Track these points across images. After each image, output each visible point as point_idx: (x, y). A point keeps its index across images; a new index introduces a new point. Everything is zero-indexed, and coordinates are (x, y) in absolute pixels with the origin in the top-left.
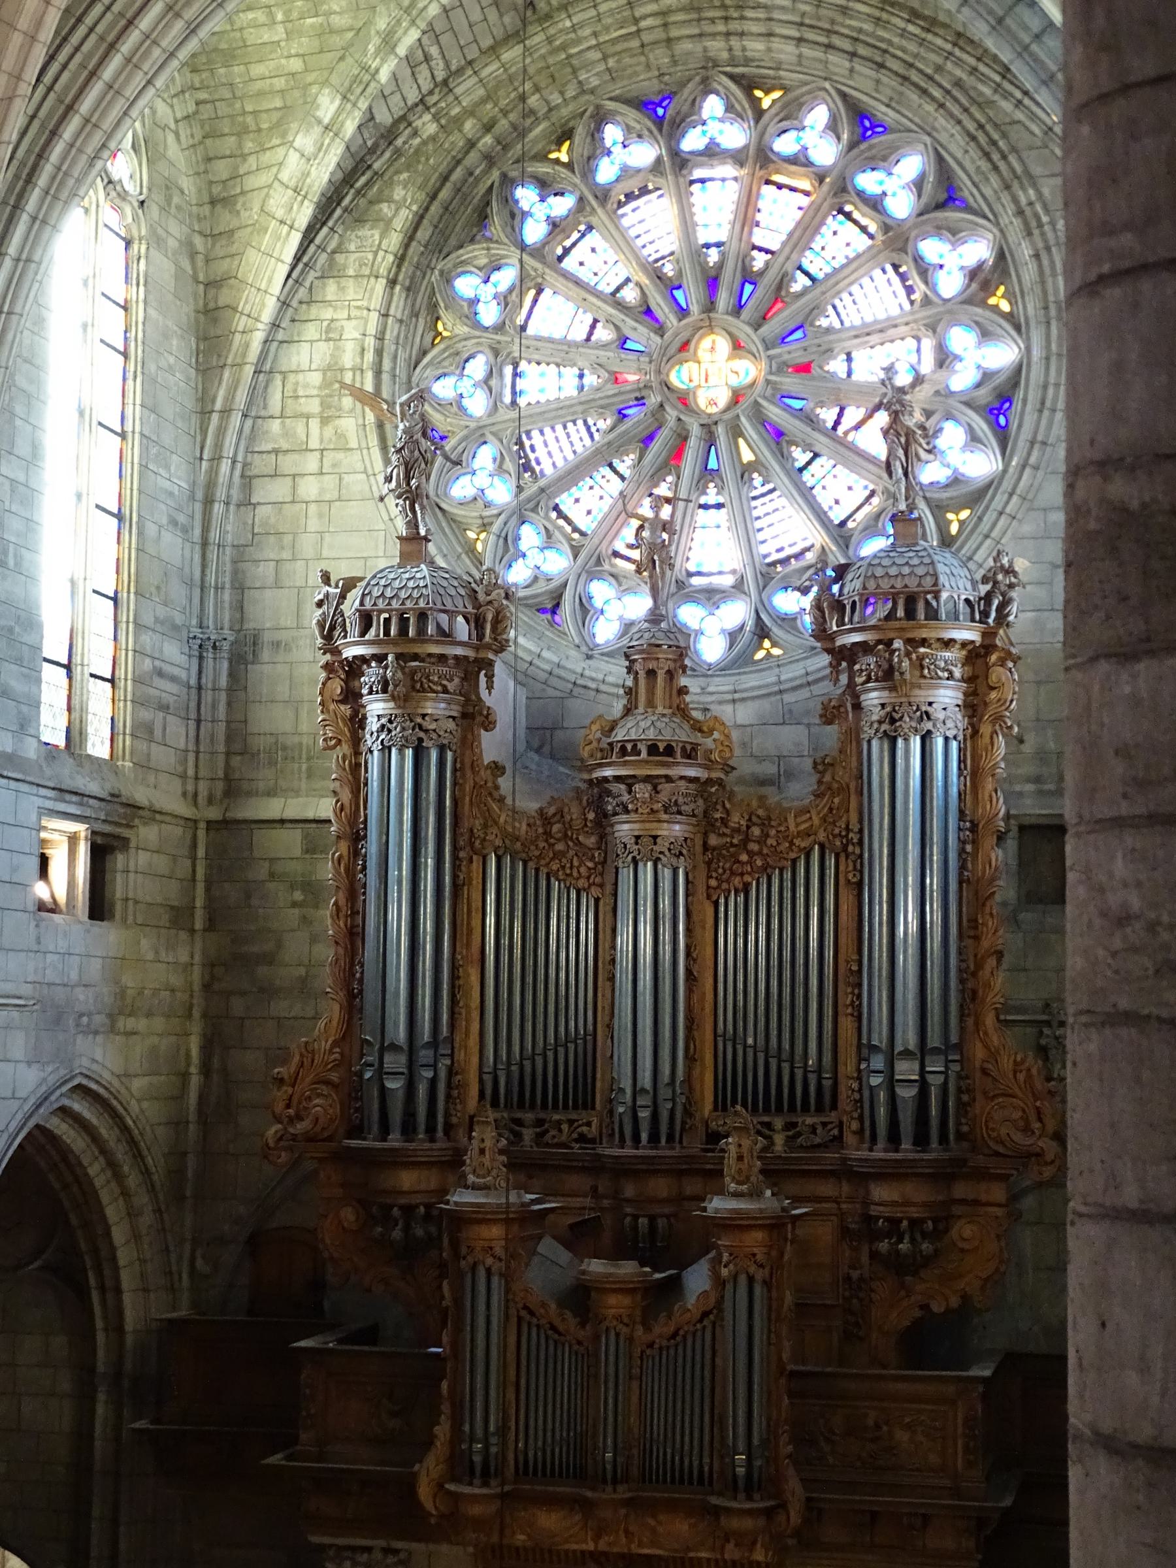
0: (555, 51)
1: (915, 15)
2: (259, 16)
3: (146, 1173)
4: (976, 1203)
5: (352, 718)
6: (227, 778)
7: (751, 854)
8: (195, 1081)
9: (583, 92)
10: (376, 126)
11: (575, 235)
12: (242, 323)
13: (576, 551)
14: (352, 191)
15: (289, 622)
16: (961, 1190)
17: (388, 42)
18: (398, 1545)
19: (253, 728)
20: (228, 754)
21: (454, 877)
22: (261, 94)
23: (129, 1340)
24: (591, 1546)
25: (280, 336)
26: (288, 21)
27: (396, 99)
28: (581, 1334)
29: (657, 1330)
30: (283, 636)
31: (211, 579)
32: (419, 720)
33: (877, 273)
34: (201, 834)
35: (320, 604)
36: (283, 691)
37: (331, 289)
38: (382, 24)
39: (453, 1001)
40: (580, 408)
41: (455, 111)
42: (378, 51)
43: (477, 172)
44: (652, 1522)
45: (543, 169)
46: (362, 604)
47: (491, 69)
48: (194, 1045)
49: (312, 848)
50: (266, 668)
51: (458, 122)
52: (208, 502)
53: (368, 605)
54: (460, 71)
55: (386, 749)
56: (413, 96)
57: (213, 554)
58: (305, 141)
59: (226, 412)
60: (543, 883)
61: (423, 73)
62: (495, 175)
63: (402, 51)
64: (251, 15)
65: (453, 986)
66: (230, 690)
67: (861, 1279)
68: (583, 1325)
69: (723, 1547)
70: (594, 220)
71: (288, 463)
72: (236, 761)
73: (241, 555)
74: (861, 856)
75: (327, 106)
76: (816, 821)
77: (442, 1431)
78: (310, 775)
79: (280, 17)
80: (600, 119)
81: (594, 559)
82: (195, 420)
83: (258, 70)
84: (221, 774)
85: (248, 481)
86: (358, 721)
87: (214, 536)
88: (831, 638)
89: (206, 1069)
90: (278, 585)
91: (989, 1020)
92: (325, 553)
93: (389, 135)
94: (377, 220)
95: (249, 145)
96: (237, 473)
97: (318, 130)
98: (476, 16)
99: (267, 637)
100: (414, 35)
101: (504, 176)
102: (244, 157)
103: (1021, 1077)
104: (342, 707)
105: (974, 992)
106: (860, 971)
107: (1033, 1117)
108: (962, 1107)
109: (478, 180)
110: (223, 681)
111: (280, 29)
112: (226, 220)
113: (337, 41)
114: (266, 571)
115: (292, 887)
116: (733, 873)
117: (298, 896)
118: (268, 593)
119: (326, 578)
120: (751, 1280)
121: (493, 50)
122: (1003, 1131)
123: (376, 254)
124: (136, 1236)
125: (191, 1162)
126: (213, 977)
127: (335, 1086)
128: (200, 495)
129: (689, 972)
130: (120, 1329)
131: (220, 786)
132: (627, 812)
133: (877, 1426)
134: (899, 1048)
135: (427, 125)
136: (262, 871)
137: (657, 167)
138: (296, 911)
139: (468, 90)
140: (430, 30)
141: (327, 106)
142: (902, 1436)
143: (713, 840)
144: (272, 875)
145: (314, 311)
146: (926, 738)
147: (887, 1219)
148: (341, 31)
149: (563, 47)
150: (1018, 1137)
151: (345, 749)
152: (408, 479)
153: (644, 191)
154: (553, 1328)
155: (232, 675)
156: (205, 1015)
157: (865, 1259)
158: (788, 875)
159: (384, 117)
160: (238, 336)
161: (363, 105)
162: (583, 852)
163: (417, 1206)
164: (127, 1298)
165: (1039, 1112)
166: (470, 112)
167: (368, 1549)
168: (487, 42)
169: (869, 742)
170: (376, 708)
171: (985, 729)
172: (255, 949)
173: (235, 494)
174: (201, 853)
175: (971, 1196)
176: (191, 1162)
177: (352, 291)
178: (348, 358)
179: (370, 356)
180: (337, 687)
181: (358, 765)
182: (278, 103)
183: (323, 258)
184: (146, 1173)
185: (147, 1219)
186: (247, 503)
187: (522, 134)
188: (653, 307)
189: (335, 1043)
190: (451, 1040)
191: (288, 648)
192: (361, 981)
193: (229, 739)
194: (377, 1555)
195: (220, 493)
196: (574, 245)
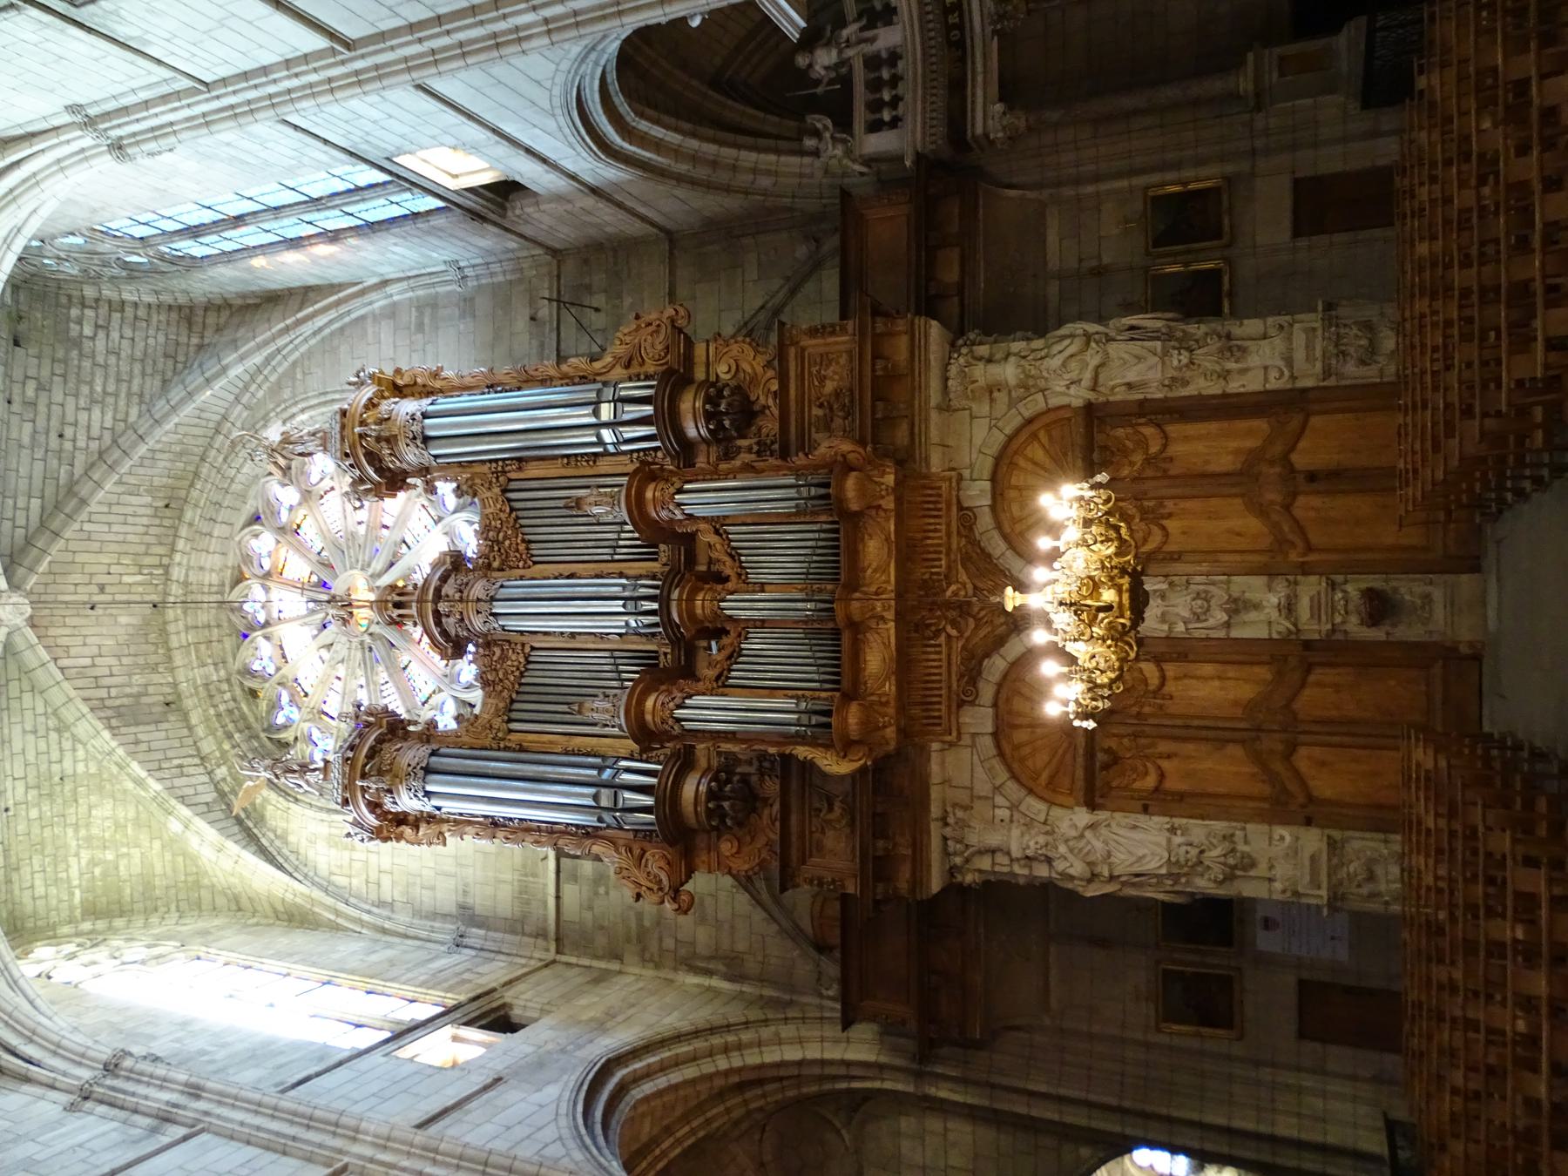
0: (197, 693)
1: (192, 485)
2: (123, 863)
3: (747, 1024)
4: (708, 365)
6: (537, 936)
7: (505, 538)
8: (715, 982)
9: (228, 681)
10: (215, 801)
12: (289, 897)
13: (440, 690)
15: (452, 881)
16: (700, 374)
17: (139, 782)
18: (935, 811)
19: (509, 915)
20: (524, 934)
21: (514, 750)
22: (174, 871)
23: (883, 1059)
24: (892, 624)
25: (311, 874)
26: (128, 845)
27: (200, 789)
28: (733, 634)
29: (728, 571)
30: (460, 888)
31: (424, 934)
33: (322, 508)
34: (564, 958)
36: (489, 890)
37: (292, 839)
38: (130, 785)
39: (588, 755)
41: (217, 754)
42: (145, 789)
44: (869, 571)
45: (263, 705)
47: (200, 731)
48: (693, 980)
49: (575, 878)
50: (478, 901)
51: (224, 753)
52: (384, 931)
54: (198, 750)
55: (428, 794)
56: (205, 779)
57: (412, 932)
58: (194, 843)
59: (338, 913)
60: (524, 689)
61: (191, 770)
62: (263, 735)
63: (144, 774)
64: (122, 868)
65: (574, 754)
66: (488, 929)
67: (758, 443)
68: (727, 633)
69: (885, 511)
70: (291, 677)
71: (373, 877)
72: (528, 929)
73: (417, 913)
74: (504, 460)
75: (175, 826)
76: (489, 494)
77: (802, 752)
78: (534, 875)
79: (124, 850)
80: (248, 672)
82: (340, 934)
83: (158, 869)
84: (532, 940)
85: (381, 904)
86: (430, 819)
87: (401, 929)
88: (377, 485)
89: (709, 973)
90: (433, 888)
91: (597, 365)
93: (222, 795)
95: (206, 881)
96: (375, 910)
97: (188, 834)
98: (163, 734)
99: (461, 899)
100: (135, 765)
101: (264, 730)
102: (213, 886)
103: (628, 339)
105: (582, 377)
106: (568, 456)
107: (650, 329)
108: (647, 378)
109: (263, 746)
110: (482, 932)
111: (132, 851)
112: (245, 903)
113: (144, 816)
114: (427, 896)
115: (596, 893)
116: (517, 550)
117: (602, 890)
118: (439, 895)
119: (349, 835)
120: (680, 491)
121: (190, 728)
122: (659, 347)
124: (801, 1041)
125: (769, 992)
126: (651, 960)
127: (644, 852)
128: (379, 936)
129: (568, 577)
130: (880, 1067)
131: (540, 942)
132: (462, 620)
133: (821, 406)
134: (593, 420)
135: (222, 772)
136: (588, 916)
137: (267, 638)
138: (612, 893)
139: (208, 746)
140: (132, 754)
141: (175, 826)
142: (830, 386)
143: (496, 564)
144: (590, 908)
145: (302, 851)
146: (425, 416)
147: (707, 423)
148: (138, 812)
149: (196, 688)
150: (662, 337)
151: (445, 827)
152: (294, 771)
153: (281, 647)
154: (730, 657)
155: (479, 927)
156: (675, 969)
157: (744, 443)
158: (520, 514)
159: (210, 797)
160: (298, 900)
161: (173, 802)
162: (504, 658)
163: (709, 789)
164: (851, 1056)
165: (650, 324)
166: (220, 745)
167: (945, 839)
168: (185, 732)
169: (436, 457)
170: (407, 802)
171: (438, 384)
172: (634, 926)
173: (385, 913)
174: (573, 960)
175: (703, 369)
176: (769, 992)
177: (293, 826)
178: (324, 830)
179: (324, 816)
180: (408, 831)
181: (455, 821)
182: (180, 859)
183: (278, 843)
184: (747, 1024)
185: (788, 1031)
186: (390, 905)
187: (243, 717)
188: (329, 642)
189: (617, 851)
190: (604, 757)
191: (466, 885)
192: (577, 826)
193: (513, 932)
194: (948, 831)
195: (379, 922)
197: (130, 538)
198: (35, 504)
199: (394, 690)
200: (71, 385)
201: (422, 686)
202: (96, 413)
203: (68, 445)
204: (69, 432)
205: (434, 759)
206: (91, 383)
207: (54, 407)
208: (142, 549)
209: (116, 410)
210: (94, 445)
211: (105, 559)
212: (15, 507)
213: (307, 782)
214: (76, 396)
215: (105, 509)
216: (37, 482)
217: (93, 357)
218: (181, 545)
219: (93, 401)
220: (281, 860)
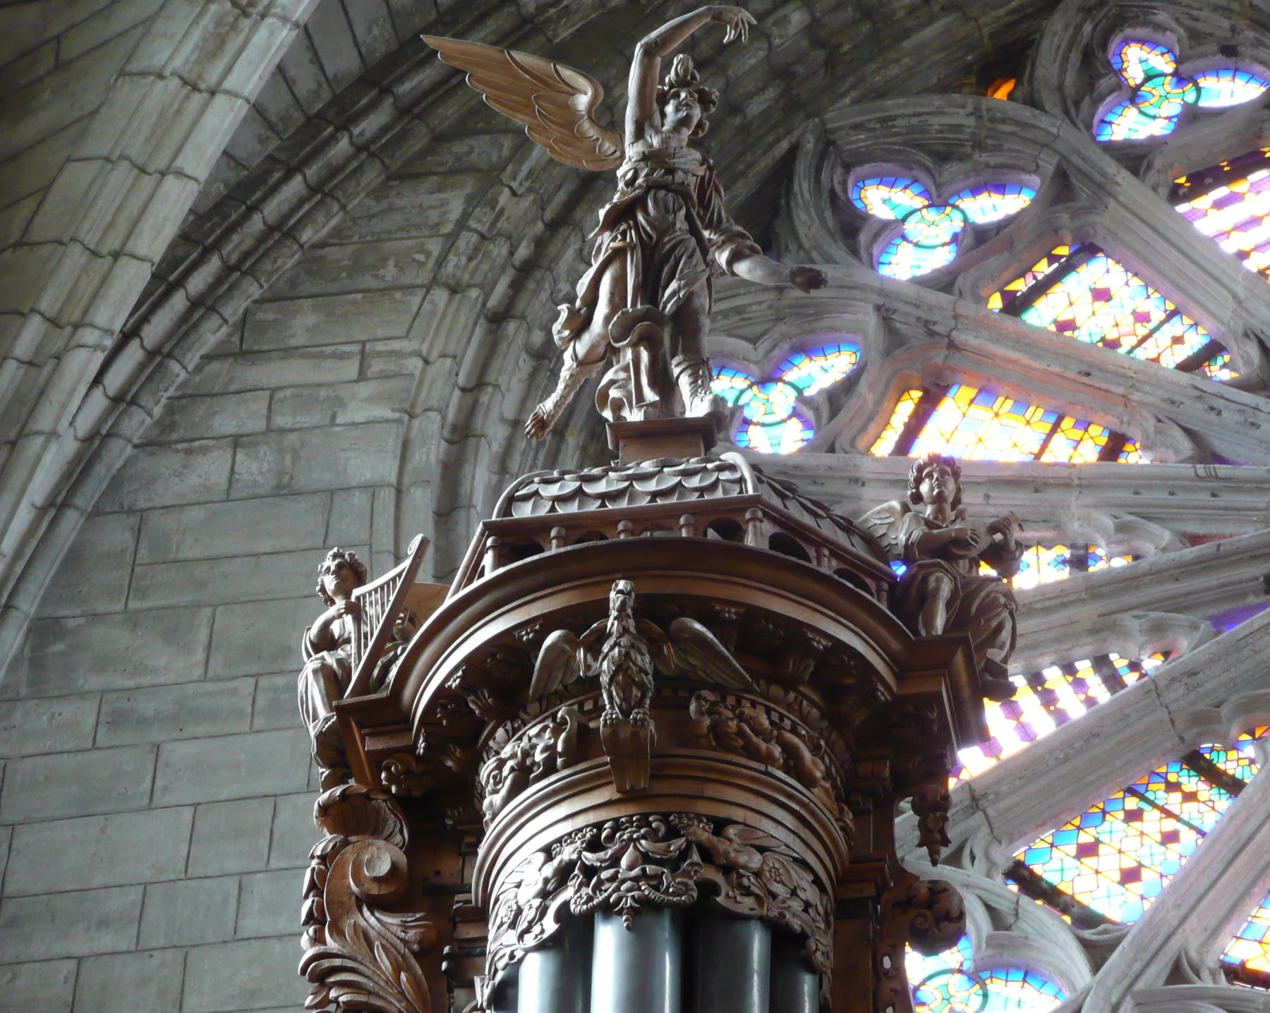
5: (426, 953)
11: (1043, 268)
13: (1097, 954)
14: (387, 105)
32: (703, 833)
35: (326, 641)
40: (1087, 613)
43: (755, 108)
46: (506, 510)
53: (524, 511)
81: (1159, 969)
92: (250, 925)
94: (452, 172)
104: (392, 920)
123: (452, 238)
152: (650, 287)
196: (1041, 288)
199: (1074, 708)
201: (1109, 862)
205: (758, 945)
213: (605, 355)
220: (198, 282)
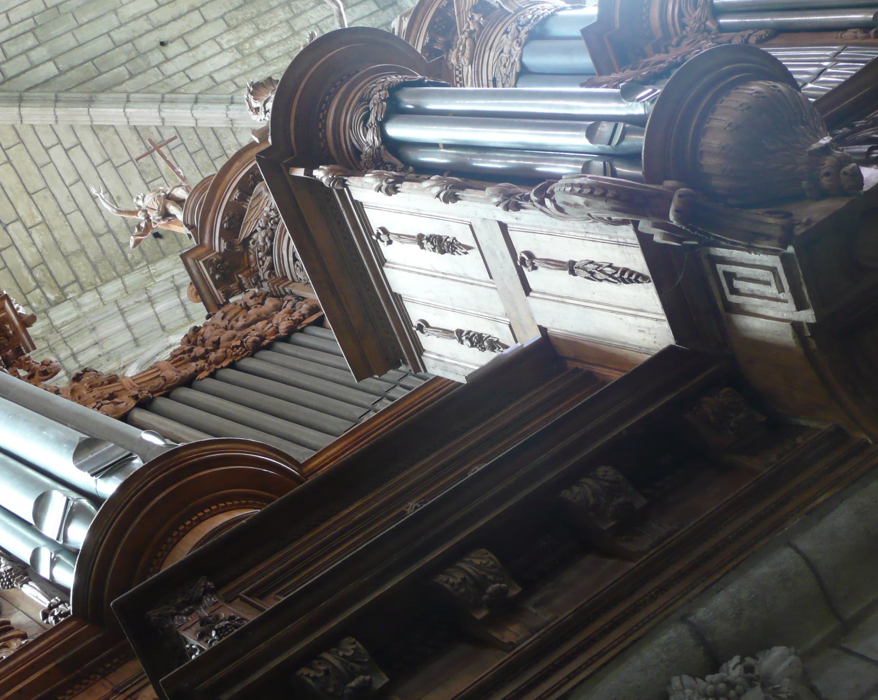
197: (76, 219)
198: (50, 69)
200: (240, 15)
202: (226, 58)
203: (156, 57)
204: (173, 49)
206: (259, 32)
207: (196, 15)
208: (70, 246)
209: (244, 73)
210: (179, 80)
211: (24, 207)
212: (25, 52)
214: (230, 28)
215: (97, 159)
216: (77, 57)
217: (296, 16)
218: (112, 289)
219: (238, 48)
